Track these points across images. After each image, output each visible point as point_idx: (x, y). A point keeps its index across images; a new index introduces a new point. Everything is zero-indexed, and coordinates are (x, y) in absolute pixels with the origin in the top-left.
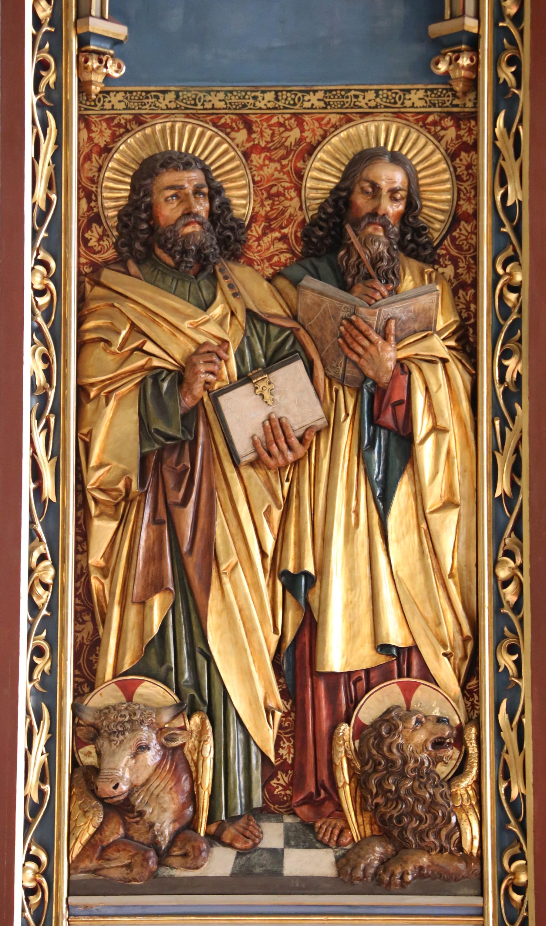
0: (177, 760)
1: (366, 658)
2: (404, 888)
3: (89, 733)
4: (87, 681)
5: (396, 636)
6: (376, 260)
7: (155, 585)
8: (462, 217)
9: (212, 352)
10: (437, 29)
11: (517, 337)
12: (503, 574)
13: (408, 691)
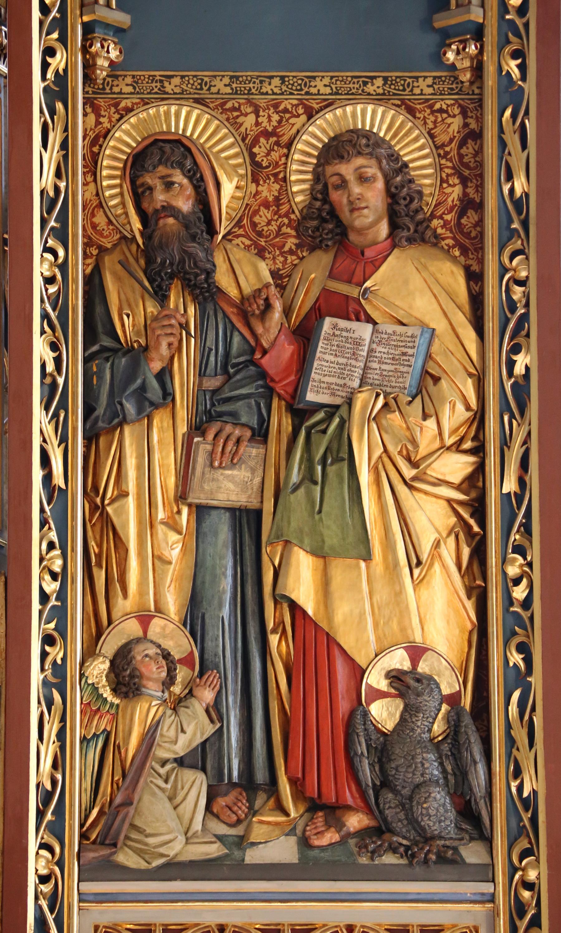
10: (442, 21)
11: (524, 333)
12: (513, 571)
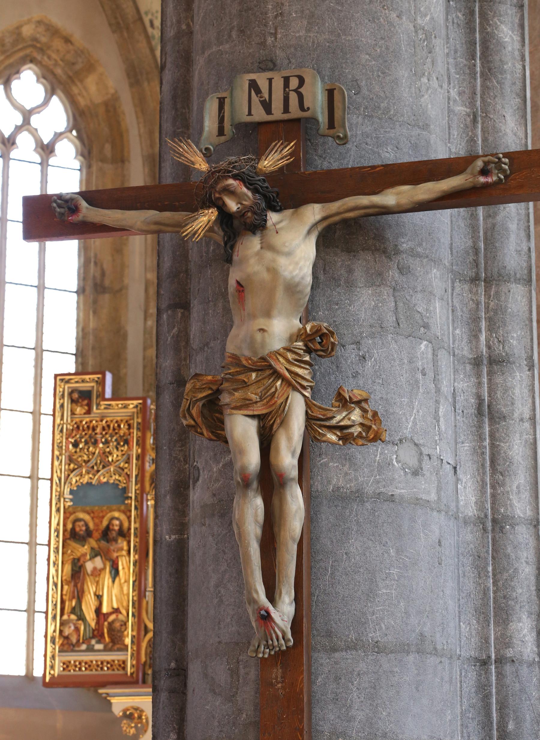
0: (77, 629)
1: (110, 610)
2: (115, 651)
3: (62, 624)
4: (62, 614)
5: (115, 606)
6: (113, 538)
7: (74, 597)
8: (129, 529)
9: (84, 555)
10: (125, 495)
13: (117, 616)
